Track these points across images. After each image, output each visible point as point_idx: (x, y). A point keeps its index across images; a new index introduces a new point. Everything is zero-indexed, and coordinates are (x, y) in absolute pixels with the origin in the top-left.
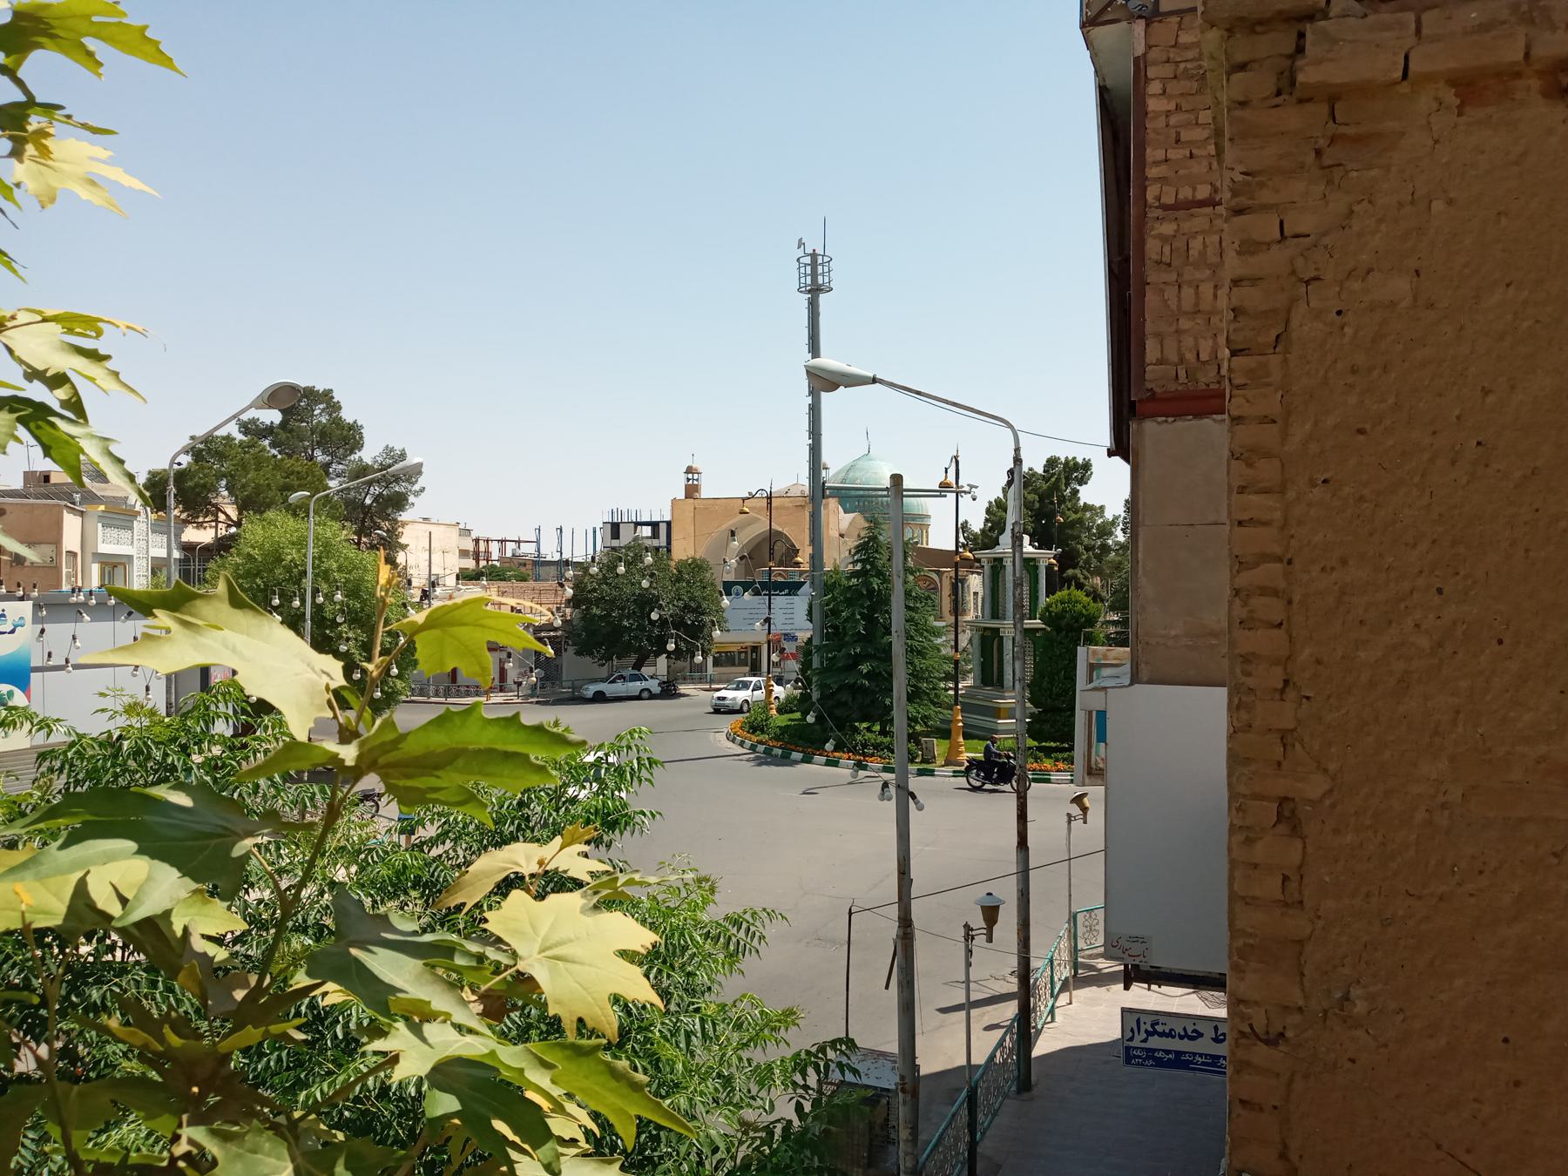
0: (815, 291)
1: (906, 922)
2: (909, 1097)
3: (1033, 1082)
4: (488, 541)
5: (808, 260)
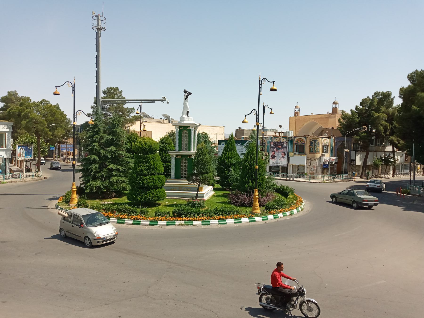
0: (99, 29)
4: (280, 133)
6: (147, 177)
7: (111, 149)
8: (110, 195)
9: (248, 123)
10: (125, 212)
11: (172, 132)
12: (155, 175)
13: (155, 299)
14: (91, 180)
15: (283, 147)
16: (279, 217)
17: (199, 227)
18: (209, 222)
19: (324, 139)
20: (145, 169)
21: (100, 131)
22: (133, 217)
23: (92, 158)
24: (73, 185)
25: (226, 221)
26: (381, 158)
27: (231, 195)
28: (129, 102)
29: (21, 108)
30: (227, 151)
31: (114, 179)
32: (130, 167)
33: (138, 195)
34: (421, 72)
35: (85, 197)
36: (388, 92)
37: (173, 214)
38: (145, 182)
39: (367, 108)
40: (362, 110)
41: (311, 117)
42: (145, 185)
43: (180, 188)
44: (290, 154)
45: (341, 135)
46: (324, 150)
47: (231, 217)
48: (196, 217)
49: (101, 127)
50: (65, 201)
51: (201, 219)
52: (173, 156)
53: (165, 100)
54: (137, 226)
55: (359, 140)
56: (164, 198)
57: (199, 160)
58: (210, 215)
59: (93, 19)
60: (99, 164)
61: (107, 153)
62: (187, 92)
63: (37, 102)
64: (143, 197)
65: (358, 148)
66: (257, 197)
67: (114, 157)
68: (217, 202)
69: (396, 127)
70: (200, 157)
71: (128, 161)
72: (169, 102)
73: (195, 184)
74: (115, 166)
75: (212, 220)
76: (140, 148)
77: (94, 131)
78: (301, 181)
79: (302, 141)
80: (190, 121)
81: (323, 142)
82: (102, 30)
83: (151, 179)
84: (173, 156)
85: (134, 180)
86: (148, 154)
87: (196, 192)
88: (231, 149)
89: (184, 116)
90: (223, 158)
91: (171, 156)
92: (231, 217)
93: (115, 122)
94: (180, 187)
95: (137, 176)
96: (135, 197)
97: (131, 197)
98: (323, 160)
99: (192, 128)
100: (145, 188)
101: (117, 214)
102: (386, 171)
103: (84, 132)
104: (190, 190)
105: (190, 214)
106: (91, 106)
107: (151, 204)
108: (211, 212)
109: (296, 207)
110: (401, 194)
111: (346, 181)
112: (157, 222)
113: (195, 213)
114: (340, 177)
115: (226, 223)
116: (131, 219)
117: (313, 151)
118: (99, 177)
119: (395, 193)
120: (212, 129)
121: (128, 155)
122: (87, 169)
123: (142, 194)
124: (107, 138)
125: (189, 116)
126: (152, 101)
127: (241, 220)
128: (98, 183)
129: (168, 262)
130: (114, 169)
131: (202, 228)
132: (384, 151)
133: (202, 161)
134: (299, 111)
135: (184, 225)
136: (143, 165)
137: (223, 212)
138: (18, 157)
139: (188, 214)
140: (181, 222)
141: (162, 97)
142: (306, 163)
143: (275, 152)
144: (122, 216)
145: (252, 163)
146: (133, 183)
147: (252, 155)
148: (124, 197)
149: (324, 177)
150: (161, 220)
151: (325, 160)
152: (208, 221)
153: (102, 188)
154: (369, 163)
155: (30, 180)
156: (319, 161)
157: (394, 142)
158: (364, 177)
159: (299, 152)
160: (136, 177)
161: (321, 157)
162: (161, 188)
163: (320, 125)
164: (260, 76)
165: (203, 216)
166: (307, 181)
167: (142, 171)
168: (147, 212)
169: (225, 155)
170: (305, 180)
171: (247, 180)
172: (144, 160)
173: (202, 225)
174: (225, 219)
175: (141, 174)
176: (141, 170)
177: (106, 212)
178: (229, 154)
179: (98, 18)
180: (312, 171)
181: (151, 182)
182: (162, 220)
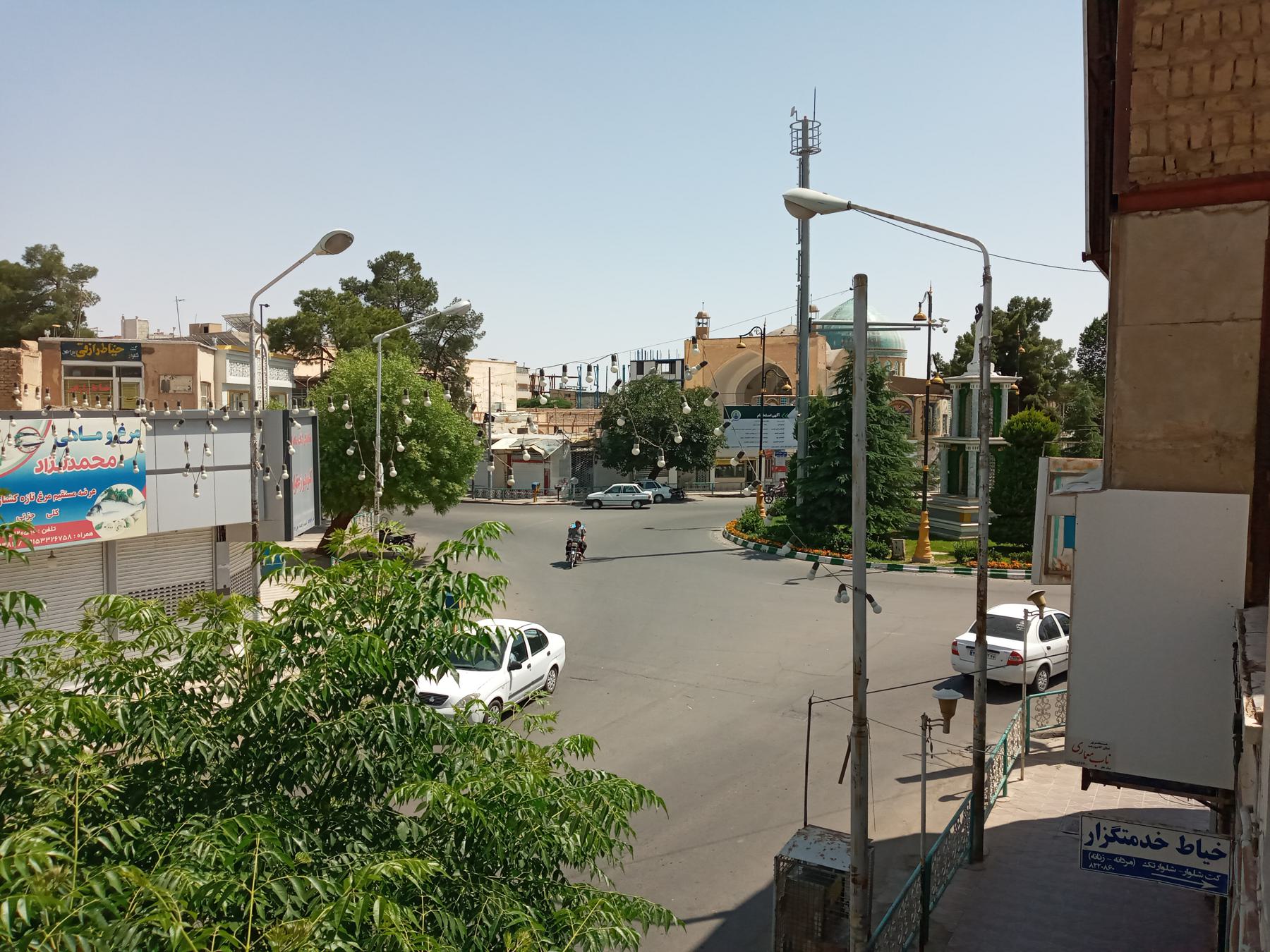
0: (805, 153)
1: (860, 721)
2: (859, 889)
3: (984, 854)
5: (799, 126)
19: (944, 400)
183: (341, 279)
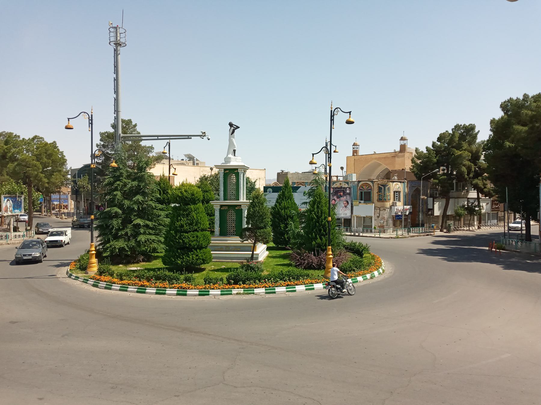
0: (118, 44)
6: (189, 235)
7: (138, 199)
8: (137, 259)
9: (316, 164)
10: (164, 280)
11: (204, 176)
12: (198, 231)
13: (237, 387)
14: (112, 240)
15: (345, 194)
16: (359, 282)
17: (262, 296)
18: (275, 289)
19: (395, 183)
20: (186, 225)
21: (122, 176)
22: (177, 286)
23: (112, 211)
24: (91, 246)
25: (295, 287)
26: (464, 206)
27: (294, 256)
28: (158, 138)
29: (6, 147)
30: (283, 200)
31: (142, 238)
32: (161, 222)
33: (178, 257)
34: (516, 100)
35: (108, 262)
36: (472, 124)
37: (227, 281)
38: (186, 240)
39: (446, 145)
40: (440, 147)
41: (374, 156)
42: (186, 244)
43: (228, 248)
44: (354, 203)
45: (415, 178)
46: (396, 198)
47: (301, 283)
48: (258, 284)
49: (123, 170)
50: (80, 268)
51: (264, 287)
52: (216, 207)
53: (205, 136)
54: (183, 297)
55: (437, 184)
56: (211, 261)
57: (255, 211)
58: (274, 280)
59: (110, 31)
60: (121, 219)
61: (132, 205)
62: (234, 126)
63: (27, 139)
64: (184, 259)
65: (436, 193)
66: (331, 256)
67: (141, 209)
68: (275, 265)
69: (481, 168)
70: (256, 207)
71: (158, 214)
72: (210, 138)
73: (249, 242)
74: (143, 221)
75: (278, 287)
76: (179, 197)
77: (115, 176)
78: (369, 237)
79: (367, 187)
80: (238, 162)
81: (394, 187)
82: (121, 45)
83: (193, 237)
84: (216, 207)
85: (171, 239)
86: (189, 205)
87: (251, 253)
88: (287, 198)
89: (230, 156)
90: (278, 209)
91: (215, 207)
92: (301, 283)
93: (141, 164)
94: (227, 246)
95: (176, 232)
96: (173, 260)
97: (168, 260)
98: (395, 209)
99: (241, 171)
100: (187, 249)
101: (154, 282)
102: (468, 222)
103: (85, 177)
104: (240, 249)
105: (250, 279)
106: (97, 144)
107: (196, 269)
108: (275, 277)
109: (377, 268)
110: (496, 250)
111: (424, 236)
112: (209, 291)
113: (256, 278)
114: (416, 230)
115: (295, 291)
116: (174, 289)
117: (382, 199)
118: (123, 235)
119: (487, 248)
120: (250, 172)
121: (159, 206)
122: (106, 225)
123: (183, 257)
124: (132, 184)
125: (236, 155)
126: (187, 137)
127: (313, 286)
128: (120, 244)
129: (238, 341)
130: (142, 224)
131: (267, 298)
132: (467, 198)
133: (259, 212)
134: (358, 149)
135: (243, 294)
136: (184, 219)
137: (290, 277)
138: (4, 211)
139: (247, 281)
140: (238, 290)
141: (201, 132)
142: (374, 214)
143: (335, 200)
144: (161, 285)
145: (320, 214)
146: (171, 242)
147: (319, 204)
148: (154, 261)
149: (397, 231)
150: (213, 289)
151: (397, 210)
152: (272, 288)
153: (127, 249)
154: (449, 213)
155: (20, 241)
156: (389, 211)
157: (480, 186)
158: (445, 230)
159: (365, 201)
160: (174, 235)
161: (392, 207)
162: (206, 247)
163: (386, 166)
164: (332, 105)
165: (266, 283)
166: (377, 236)
167: (182, 226)
168: (194, 279)
169: (280, 205)
170: (373, 235)
171: (314, 236)
172: (185, 212)
173: (266, 293)
174: (294, 285)
175: (181, 230)
176: (180, 225)
177: (140, 280)
178: (284, 203)
179: (116, 30)
180: (382, 224)
181: (195, 240)
182: (214, 289)
183: (100, 132)
